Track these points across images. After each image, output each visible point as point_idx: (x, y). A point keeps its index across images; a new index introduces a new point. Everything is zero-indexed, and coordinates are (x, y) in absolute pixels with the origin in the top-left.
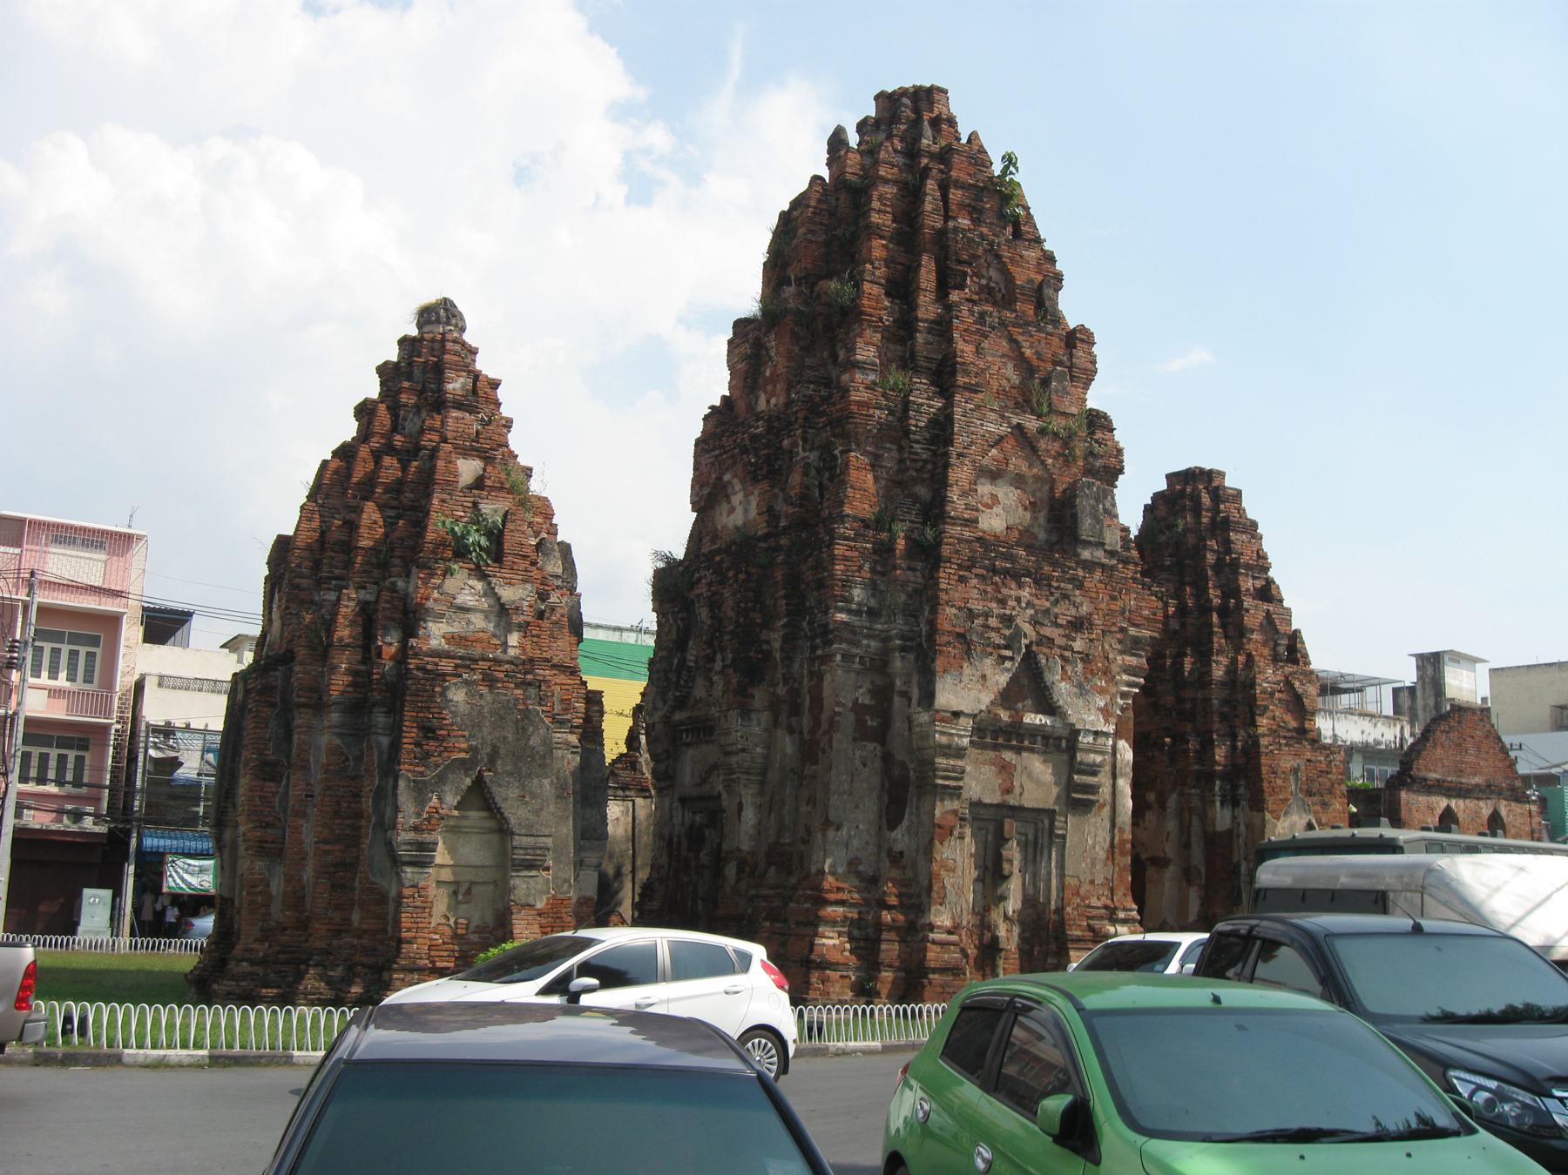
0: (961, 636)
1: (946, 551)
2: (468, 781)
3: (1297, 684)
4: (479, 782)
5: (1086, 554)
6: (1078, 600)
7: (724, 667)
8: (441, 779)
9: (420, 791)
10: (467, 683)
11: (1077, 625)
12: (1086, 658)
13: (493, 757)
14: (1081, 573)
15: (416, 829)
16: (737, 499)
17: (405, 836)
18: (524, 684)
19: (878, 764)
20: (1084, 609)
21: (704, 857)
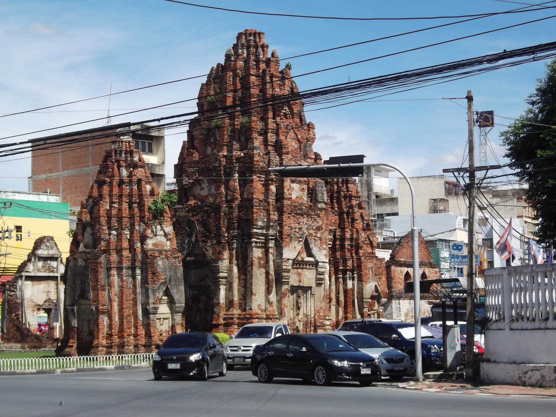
0: (289, 235)
1: (285, 209)
2: (165, 288)
3: (371, 238)
4: (167, 288)
5: (320, 206)
6: (319, 221)
7: (212, 245)
8: (159, 288)
9: (154, 291)
10: (161, 258)
11: (319, 229)
12: (320, 239)
13: (170, 280)
14: (319, 212)
15: (154, 303)
16: (205, 185)
17: (152, 306)
18: (175, 258)
19: (264, 275)
20: (320, 224)
21: (201, 305)
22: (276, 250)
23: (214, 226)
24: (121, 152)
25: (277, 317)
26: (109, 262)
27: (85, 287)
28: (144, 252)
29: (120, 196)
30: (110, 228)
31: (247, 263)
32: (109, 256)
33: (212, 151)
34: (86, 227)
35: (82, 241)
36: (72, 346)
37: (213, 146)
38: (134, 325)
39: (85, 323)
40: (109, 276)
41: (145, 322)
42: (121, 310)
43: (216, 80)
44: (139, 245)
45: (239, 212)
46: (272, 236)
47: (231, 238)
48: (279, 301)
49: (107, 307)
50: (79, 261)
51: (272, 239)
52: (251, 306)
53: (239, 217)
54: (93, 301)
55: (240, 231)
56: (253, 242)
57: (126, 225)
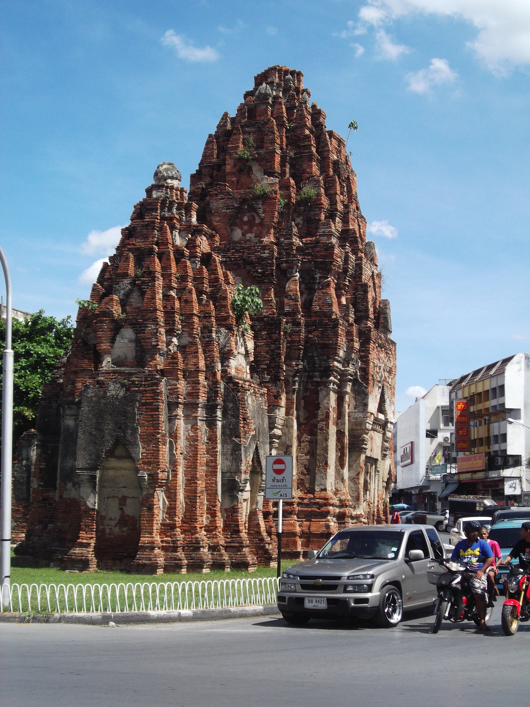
22: (355, 398)
23: (267, 353)
24: (172, 203)
25: (351, 503)
26: (173, 391)
27: (125, 436)
28: (229, 379)
29: (183, 278)
30: (170, 332)
31: (316, 416)
32: (174, 382)
33: (243, 235)
34: (122, 327)
35: (108, 352)
36: (88, 545)
37: (246, 227)
38: (208, 509)
39: (114, 504)
40: (171, 419)
41: (227, 505)
42: (191, 481)
43: (247, 129)
44: (219, 366)
45: (308, 332)
46: (351, 376)
47: (291, 374)
48: (354, 480)
49: (166, 474)
50: (112, 387)
51: (350, 380)
52: (325, 486)
53: (307, 340)
54: (144, 463)
55: (305, 363)
56: (331, 381)
57: (197, 329)
